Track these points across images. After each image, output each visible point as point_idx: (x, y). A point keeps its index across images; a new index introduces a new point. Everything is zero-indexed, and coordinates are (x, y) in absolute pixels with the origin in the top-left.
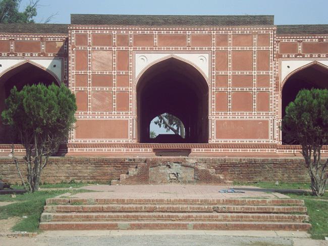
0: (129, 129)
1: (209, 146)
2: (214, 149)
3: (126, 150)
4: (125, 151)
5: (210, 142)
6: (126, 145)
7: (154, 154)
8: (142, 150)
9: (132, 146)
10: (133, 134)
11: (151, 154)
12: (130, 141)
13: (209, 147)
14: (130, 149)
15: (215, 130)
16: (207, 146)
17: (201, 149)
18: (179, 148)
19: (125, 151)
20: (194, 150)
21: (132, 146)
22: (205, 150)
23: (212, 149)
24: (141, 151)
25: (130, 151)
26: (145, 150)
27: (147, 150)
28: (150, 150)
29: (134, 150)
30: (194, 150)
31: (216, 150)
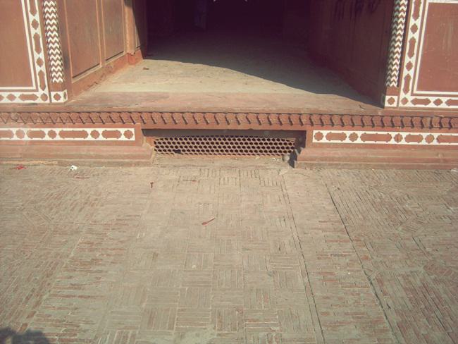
0: (30, 44)
1: (387, 121)
2: (404, 134)
3: (32, 134)
4: (26, 138)
5: (393, 102)
6: (26, 115)
7: (148, 145)
8: (95, 134)
9: (50, 116)
10: (48, 67)
11: (135, 150)
12: (40, 95)
13: (383, 127)
14: (46, 130)
15: (419, 49)
16: (377, 121)
17: (348, 133)
18: (255, 126)
19: (26, 138)
20: (319, 136)
21: (50, 116)
22: (364, 137)
23: (393, 134)
24: (90, 138)
25: (47, 138)
26: (106, 134)
27: (117, 134)
28: (128, 134)
29: (62, 134)
30: (319, 136)
31: (409, 138)
